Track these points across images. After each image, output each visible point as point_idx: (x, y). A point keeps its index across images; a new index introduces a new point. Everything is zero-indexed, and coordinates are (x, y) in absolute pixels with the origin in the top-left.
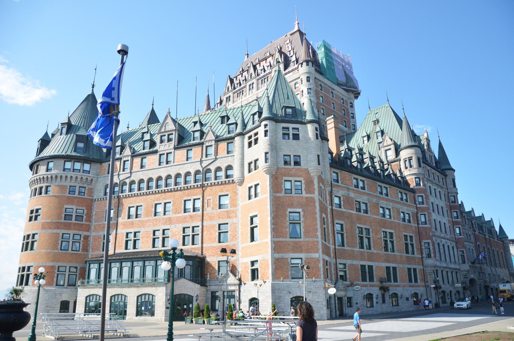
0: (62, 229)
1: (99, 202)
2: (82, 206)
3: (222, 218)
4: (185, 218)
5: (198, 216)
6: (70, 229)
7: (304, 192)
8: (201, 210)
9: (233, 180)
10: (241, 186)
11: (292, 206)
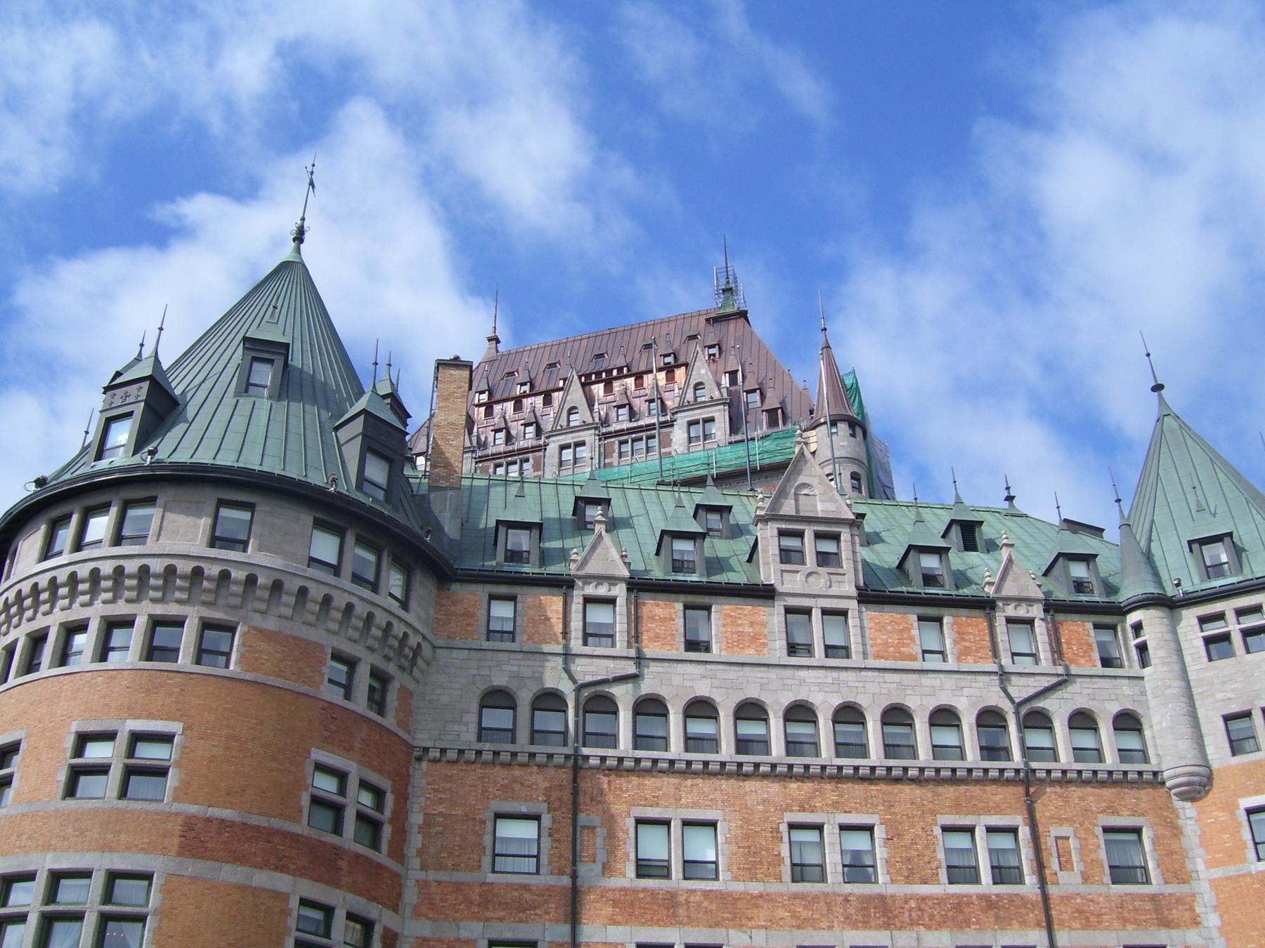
0: (300, 872)
1: (443, 769)
2: (380, 771)
3: (1136, 922)
4: (960, 904)
5: (1025, 906)
6: (334, 883)
8: (1030, 879)
9: (1155, 774)
10: (1193, 800)
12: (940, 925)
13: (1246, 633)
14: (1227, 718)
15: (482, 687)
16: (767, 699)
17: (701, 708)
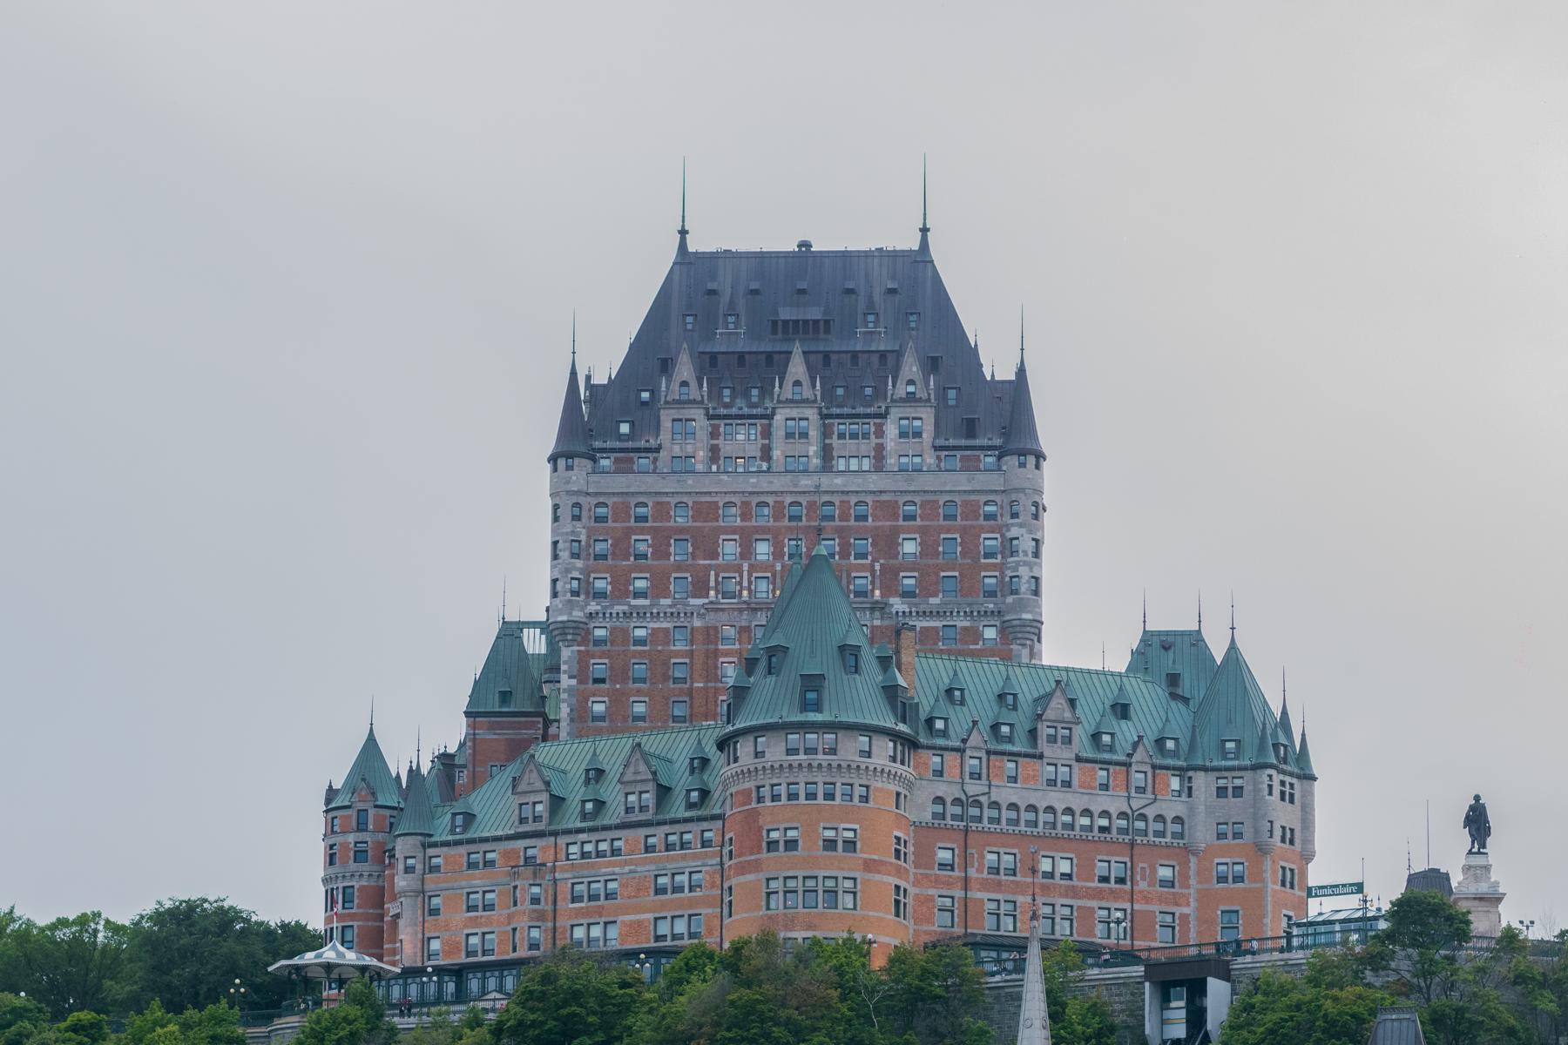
4: (1101, 890)
6: (900, 878)
7: (1296, 887)
8: (1129, 883)
9: (1184, 844)
11: (1285, 906)
12: (1093, 899)
13: (1234, 788)
14: (1218, 824)
15: (932, 797)
16: (1038, 805)
17: (1013, 806)
